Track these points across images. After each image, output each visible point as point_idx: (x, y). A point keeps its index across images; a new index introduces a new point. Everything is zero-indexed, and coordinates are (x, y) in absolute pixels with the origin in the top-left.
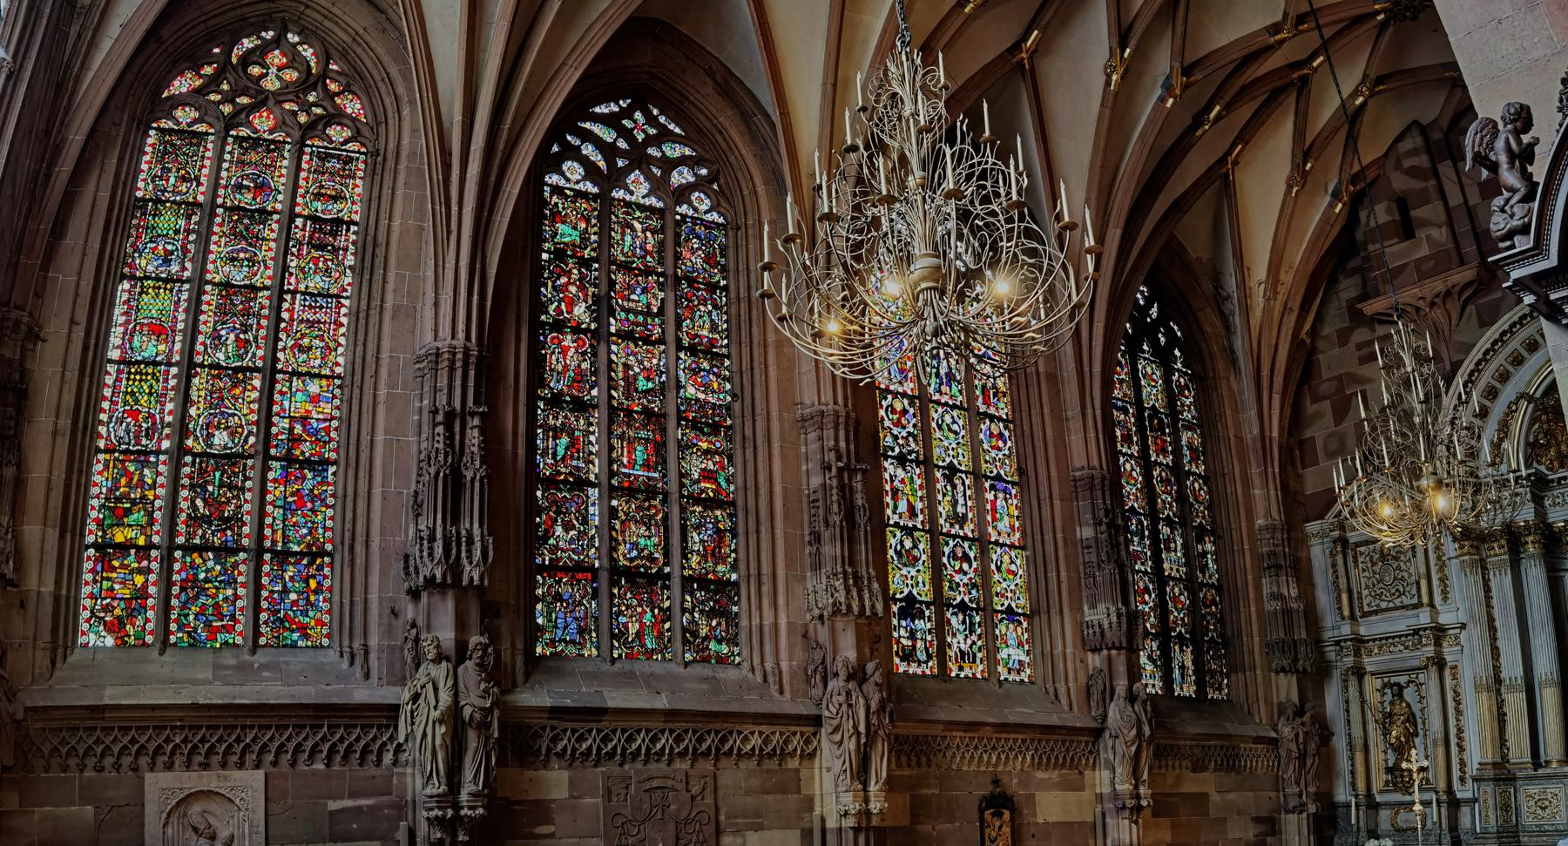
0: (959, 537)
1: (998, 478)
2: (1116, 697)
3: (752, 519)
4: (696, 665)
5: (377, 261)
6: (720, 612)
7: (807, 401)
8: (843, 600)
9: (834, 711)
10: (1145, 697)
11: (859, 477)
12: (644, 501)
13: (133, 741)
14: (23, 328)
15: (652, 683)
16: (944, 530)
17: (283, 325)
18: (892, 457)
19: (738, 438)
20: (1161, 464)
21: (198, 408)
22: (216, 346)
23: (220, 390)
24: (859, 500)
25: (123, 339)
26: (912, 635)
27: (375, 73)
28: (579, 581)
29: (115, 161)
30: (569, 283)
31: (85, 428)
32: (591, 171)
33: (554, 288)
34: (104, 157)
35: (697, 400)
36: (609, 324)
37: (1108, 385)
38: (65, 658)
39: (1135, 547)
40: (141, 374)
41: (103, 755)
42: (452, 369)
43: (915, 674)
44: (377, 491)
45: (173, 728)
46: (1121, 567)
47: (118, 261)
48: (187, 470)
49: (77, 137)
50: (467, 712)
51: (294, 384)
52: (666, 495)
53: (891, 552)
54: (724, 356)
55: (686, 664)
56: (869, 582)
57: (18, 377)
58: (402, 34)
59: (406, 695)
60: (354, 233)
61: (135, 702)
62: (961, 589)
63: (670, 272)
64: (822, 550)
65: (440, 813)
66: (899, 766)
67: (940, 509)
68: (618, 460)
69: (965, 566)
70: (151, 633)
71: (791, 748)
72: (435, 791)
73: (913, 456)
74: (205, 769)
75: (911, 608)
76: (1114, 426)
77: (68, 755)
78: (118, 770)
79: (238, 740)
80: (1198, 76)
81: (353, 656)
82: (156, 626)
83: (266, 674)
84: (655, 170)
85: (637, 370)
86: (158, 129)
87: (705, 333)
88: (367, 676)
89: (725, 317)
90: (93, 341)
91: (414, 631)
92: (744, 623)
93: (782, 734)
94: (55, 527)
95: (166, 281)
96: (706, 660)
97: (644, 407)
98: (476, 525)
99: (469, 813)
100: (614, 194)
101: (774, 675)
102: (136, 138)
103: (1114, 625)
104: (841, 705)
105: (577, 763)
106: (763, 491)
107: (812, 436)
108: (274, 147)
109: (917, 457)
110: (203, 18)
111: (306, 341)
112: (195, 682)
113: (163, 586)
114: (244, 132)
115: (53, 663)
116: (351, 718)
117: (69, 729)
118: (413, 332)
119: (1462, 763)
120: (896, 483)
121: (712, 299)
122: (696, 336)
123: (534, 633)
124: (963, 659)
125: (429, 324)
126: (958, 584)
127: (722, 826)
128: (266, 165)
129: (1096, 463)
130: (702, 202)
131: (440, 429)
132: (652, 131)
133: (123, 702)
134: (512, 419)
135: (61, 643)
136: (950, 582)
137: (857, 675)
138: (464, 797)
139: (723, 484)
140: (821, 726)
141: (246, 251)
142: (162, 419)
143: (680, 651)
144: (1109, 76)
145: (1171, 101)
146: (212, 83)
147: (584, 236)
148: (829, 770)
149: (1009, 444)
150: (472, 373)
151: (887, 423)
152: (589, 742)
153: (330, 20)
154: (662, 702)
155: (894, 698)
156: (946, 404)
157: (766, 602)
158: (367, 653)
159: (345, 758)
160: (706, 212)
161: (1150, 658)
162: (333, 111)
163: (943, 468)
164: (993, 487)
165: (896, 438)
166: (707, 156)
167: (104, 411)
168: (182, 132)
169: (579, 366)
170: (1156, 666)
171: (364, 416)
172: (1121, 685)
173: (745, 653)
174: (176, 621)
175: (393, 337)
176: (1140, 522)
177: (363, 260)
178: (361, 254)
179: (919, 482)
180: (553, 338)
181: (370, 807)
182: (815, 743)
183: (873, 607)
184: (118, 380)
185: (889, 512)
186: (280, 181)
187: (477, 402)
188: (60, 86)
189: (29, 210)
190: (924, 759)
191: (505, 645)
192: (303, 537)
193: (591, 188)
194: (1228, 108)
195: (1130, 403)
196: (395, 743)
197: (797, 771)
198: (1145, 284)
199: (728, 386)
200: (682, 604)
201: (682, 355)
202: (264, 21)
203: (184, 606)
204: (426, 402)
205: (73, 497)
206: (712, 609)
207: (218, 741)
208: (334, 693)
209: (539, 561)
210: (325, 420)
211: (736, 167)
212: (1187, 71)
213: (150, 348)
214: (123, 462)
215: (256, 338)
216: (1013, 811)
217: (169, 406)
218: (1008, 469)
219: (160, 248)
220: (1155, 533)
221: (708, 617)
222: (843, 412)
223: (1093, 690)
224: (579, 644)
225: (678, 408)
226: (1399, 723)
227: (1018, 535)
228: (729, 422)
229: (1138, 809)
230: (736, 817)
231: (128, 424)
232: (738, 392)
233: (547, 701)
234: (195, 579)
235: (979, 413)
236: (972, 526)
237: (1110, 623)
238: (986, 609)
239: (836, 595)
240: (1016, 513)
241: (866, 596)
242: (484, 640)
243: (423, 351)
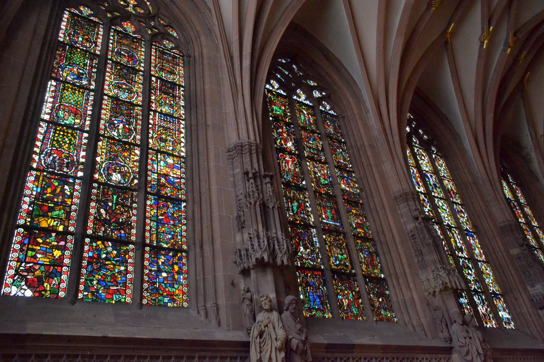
21: (102, 158)
35: (347, 191)
48: (94, 191)
51: (159, 156)
88: (219, 324)
92: (394, 299)
96: (382, 320)
97: (326, 192)
157: (403, 288)
167: (38, 147)
180: (281, 155)
203: (91, 274)
221: (377, 296)
231: (54, 158)
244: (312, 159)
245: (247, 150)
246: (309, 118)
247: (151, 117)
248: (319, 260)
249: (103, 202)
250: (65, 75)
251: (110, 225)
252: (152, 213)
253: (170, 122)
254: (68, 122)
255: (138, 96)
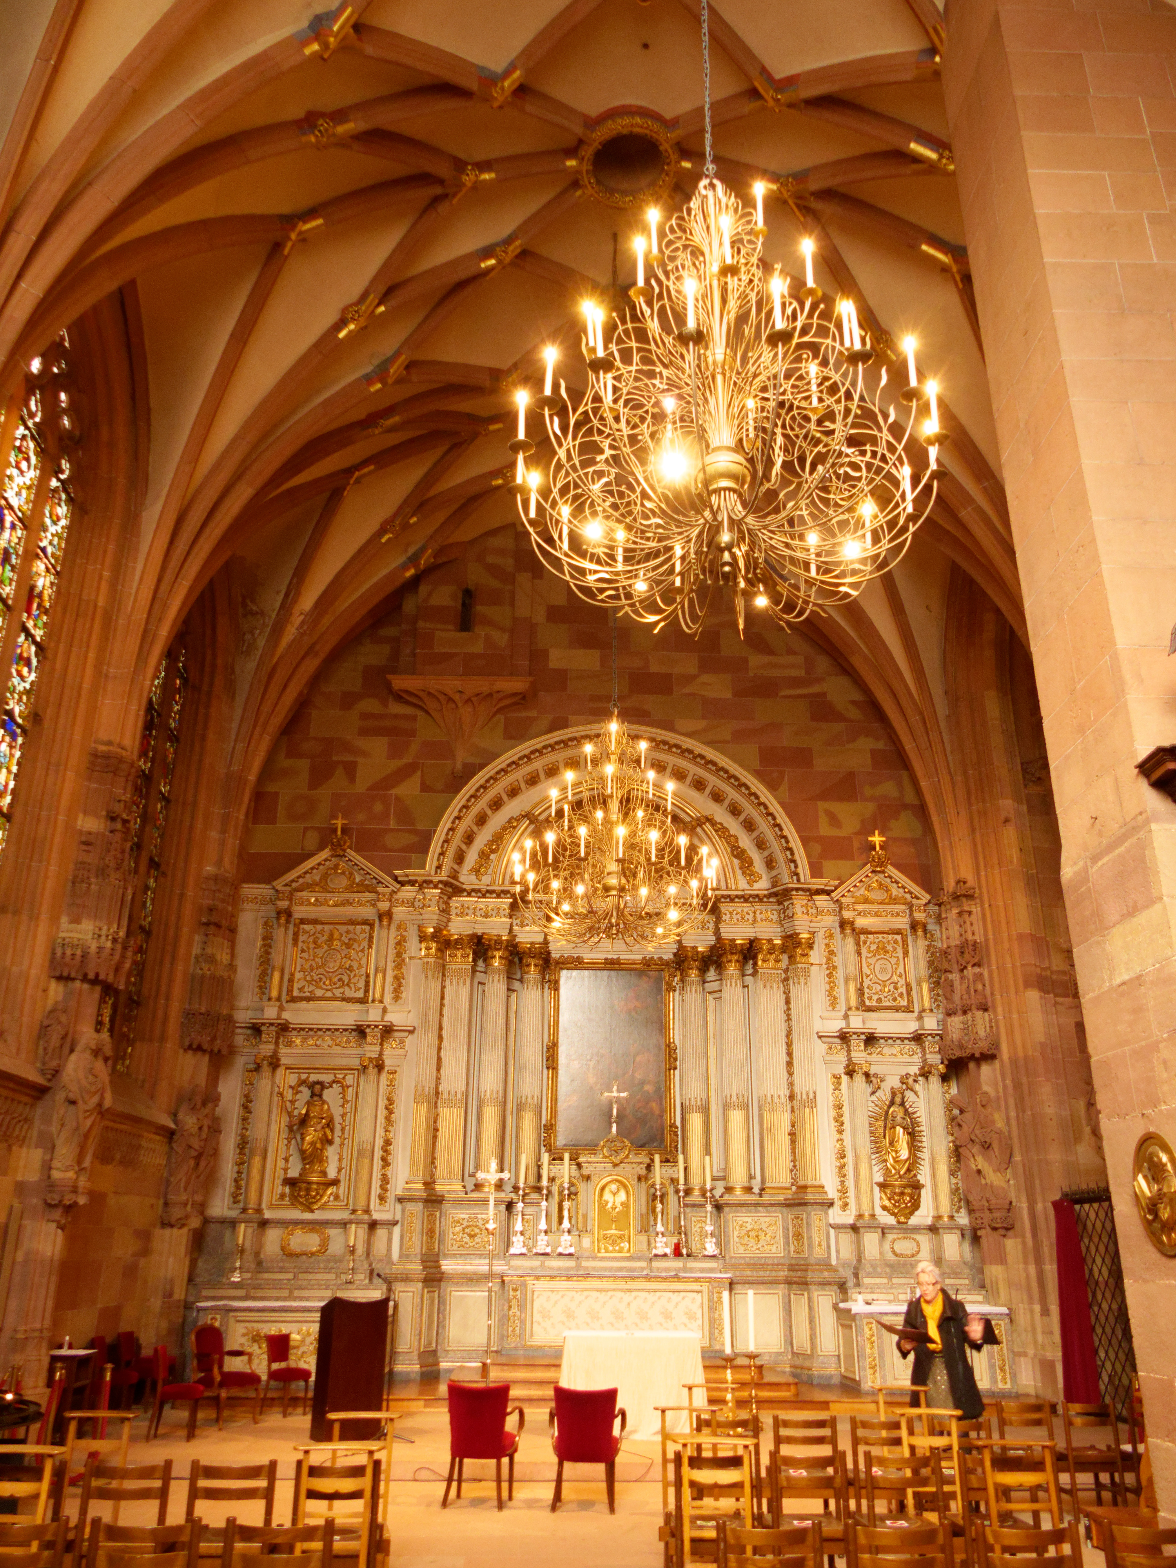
119: (385, 1180)
226: (319, 1127)
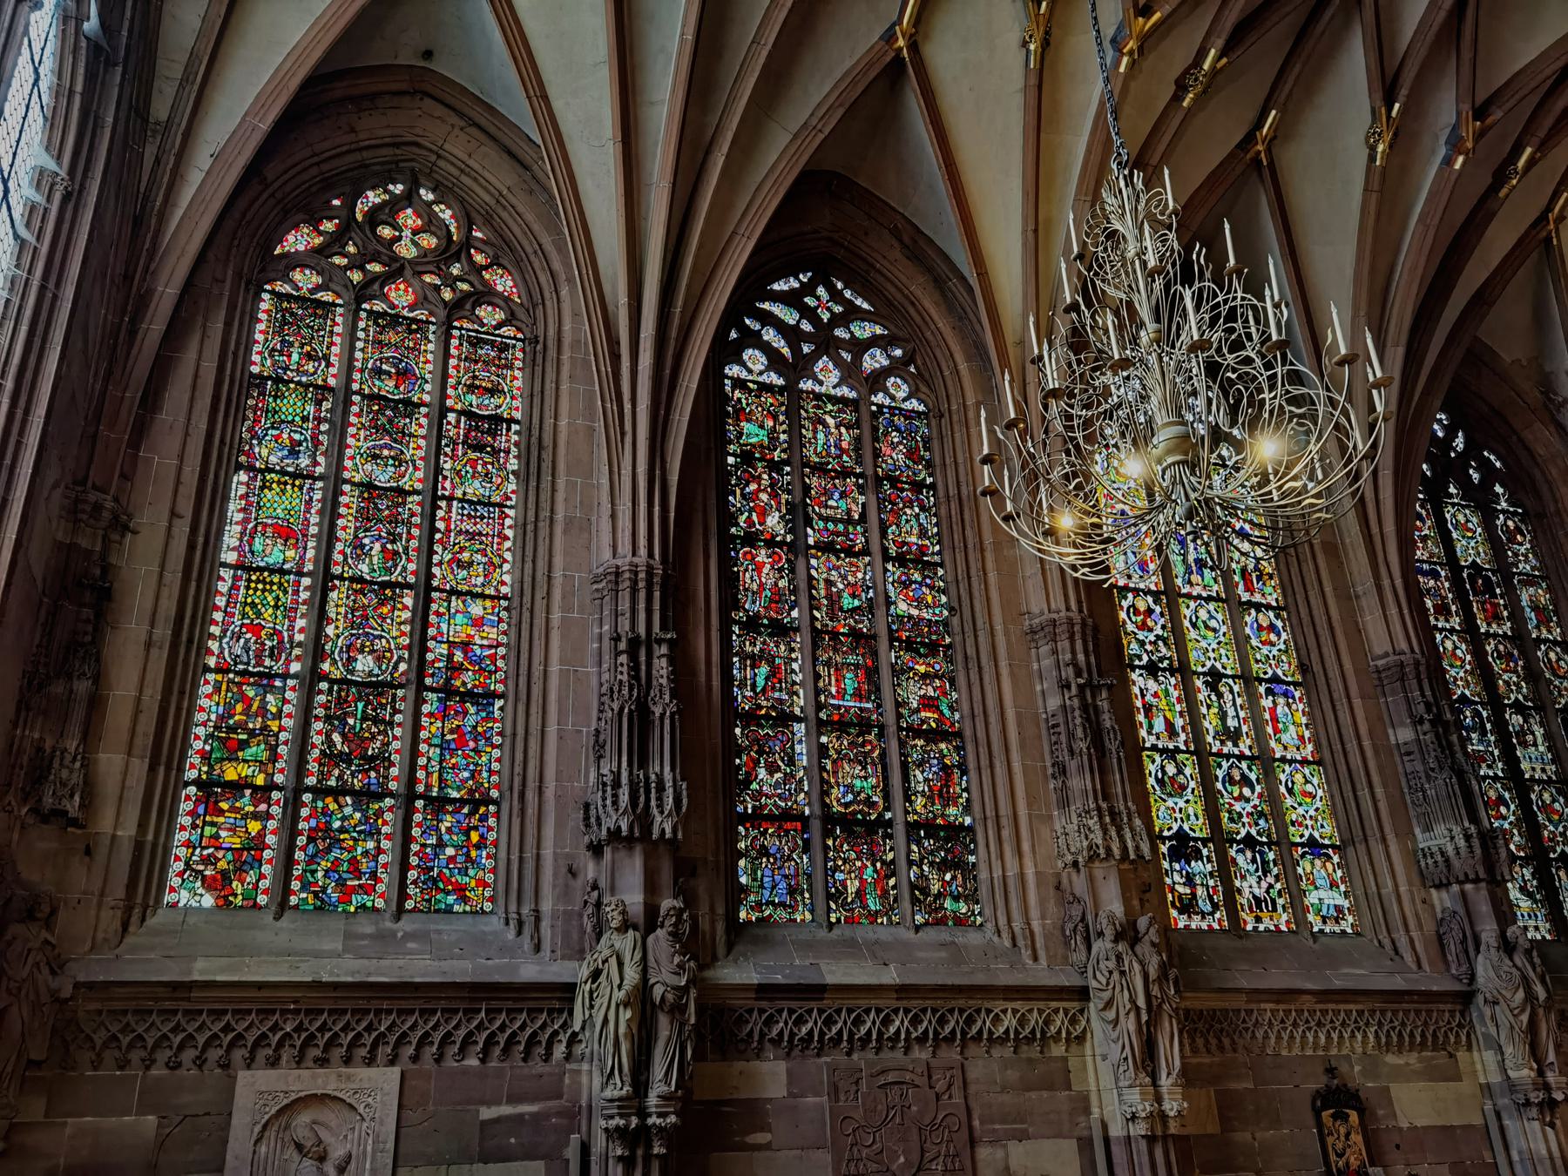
0: (1234, 756)
1: (1275, 679)
2: (1483, 948)
3: (983, 751)
4: (928, 929)
5: (544, 465)
6: (955, 864)
7: (1036, 610)
8: (1100, 842)
9: (1104, 981)
10: (1527, 945)
11: (1104, 694)
12: (858, 736)
13: (227, 1029)
14: (106, 514)
15: (878, 952)
16: (1214, 750)
17: (438, 536)
18: (1141, 667)
19: (960, 658)
20: (1495, 636)
22: (358, 556)
23: (364, 607)
24: (1107, 721)
25: (241, 540)
26: (1189, 880)
27: (525, 243)
28: (787, 832)
29: (220, 325)
30: (759, 490)
31: (190, 641)
32: (774, 359)
33: (743, 496)
34: (206, 319)
35: (910, 617)
36: (806, 536)
37: (1406, 545)
38: (143, 920)
39: (1475, 746)
40: (264, 582)
41: (181, 1047)
42: (634, 591)
43: (1200, 930)
44: (552, 729)
45: (284, 1012)
46: (1460, 774)
47: (231, 447)
48: (322, 698)
49: (168, 290)
50: (658, 991)
51: (453, 604)
52: (882, 728)
53: (1151, 781)
54: (936, 564)
55: (917, 928)
56: (1130, 819)
57: (98, 572)
58: (552, 198)
59: (585, 972)
60: (516, 433)
61: (236, 979)
62: (1245, 820)
63: (870, 472)
64: (1069, 784)
65: (622, 1122)
66: (1195, 1051)
67: (1206, 724)
68: (826, 690)
69: (1246, 791)
70: (265, 892)
71: (1053, 1030)
72: (617, 1094)
73: (1165, 664)
74: (321, 1066)
75: (1183, 847)
76: (1422, 596)
77: (131, 1046)
78: (200, 1067)
79: (369, 1029)
80: (1497, 115)
81: (520, 924)
82: (273, 884)
83: (411, 945)
84: (844, 355)
85: (841, 586)
86: (272, 292)
87: (913, 539)
89: (934, 520)
90: (201, 540)
91: (595, 894)
92: (983, 875)
93: (1040, 1012)
94: (142, 757)
95: (294, 476)
96: (941, 922)
97: (851, 628)
98: (667, 769)
99: (658, 1121)
100: (801, 385)
101: (1025, 938)
102: (245, 300)
103: (1463, 851)
104: (1111, 973)
105: (796, 1052)
106: (994, 719)
107: (1045, 649)
108: (416, 327)
109: (1171, 665)
110: (316, 159)
111: (466, 556)
112: (318, 955)
113: (286, 835)
114: (379, 306)
115: (125, 926)
116: (515, 1000)
117: (136, 1012)
118: (588, 548)
120: (1148, 698)
121: (918, 499)
122: (904, 543)
123: (736, 894)
124: (1259, 907)
125: (606, 539)
126: (1240, 815)
127: (977, 1133)
128: (408, 348)
129: (1404, 646)
130: (898, 388)
131: (623, 659)
132: (838, 309)
133: (219, 978)
134: (705, 645)
135: (139, 900)
136: (1230, 812)
137: (1128, 934)
138: (652, 1100)
139: (946, 712)
140: (1088, 999)
141: (391, 448)
142: (291, 637)
143: (909, 912)
144: (1373, 149)
145: (1461, 159)
146: (334, 243)
147: (773, 435)
148: (1104, 1058)
149: (1284, 636)
150: (657, 594)
151: (1130, 627)
152: (810, 1025)
153: (468, 175)
154: (890, 976)
155: (1176, 960)
156: (1199, 597)
158: (538, 919)
159: (506, 1051)
160: (904, 400)
161: (1523, 890)
162: (481, 288)
163: (1204, 674)
164: (1269, 692)
165: (1142, 643)
166: (901, 334)
168: (301, 300)
169: (776, 584)
170: (1535, 901)
171: (536, 642)
172: (1488, 931)
173: (988, 912)
174: (299, 878)
175: (566, 553)
176: (1477, 714)
177: (528, 464)
178: (524, 457)
179: (1176, 694)
180: (745, 554)
181: (533, 1115)
182: (1084, 1023)
183: (1137, 848)
184: (234, 587)
185: (1143, 733)
186: (426, 367)
187: (664, 628)
188: (138, 222)
189: (109, 374)
190: (1226, 1041)
191: (704, 909)
192: (464, 781)
193: (775, 379)
194: (1543, 147)
195: (1441, 564)
196: (569, 1032)
197: (1065, 1059)
198: (1442, 410)
199: (944, 599)
200: (908, 855)
201: (890, 566)
202: (389, 171)
204: (606, 628)
205: (170, 723)
206: (944, 860)
207: (342, 1029)
208: (494, 969)
209: (740, 809)
210: (490, 647)
211: (933, 343)
212: (1480, 113)
213: (276, 554)
214: (239, 685)
215: (406, 549)
216: (1361, 1112)
217: (301, 623)
218: (1286, 667)
219: (285, 436)
220: (1501, 726)
221: (939, 869)
222: (1077, 618)
223: (1448, 939)
224: (790, 906)
225: (889, 627)
227: (1310, 747)
228: (948, 640)
229: (1550, 1105)
230: (993, 1122)
232: (956, 605)
233: (754, 978)
234: (328, 828)
235: (1241, 604)
236: (1248, 742)
237: (1457, 849)
238: (1281, 842)
239: (1091, 836)
240: (1304, 720)
241: (1128, 836)
242: (679, 904)
243: (601, 570)
244: (826, 548)
245: (627, 583)
246: (841, 434)
247: (440, 513)
248: (802, 795)
249: (337, 718)
250: (265, 452)
251: (350, 763)
252: (433, 730)
253: (482, 517)
254: (271, 561)
255: (416, 469)
